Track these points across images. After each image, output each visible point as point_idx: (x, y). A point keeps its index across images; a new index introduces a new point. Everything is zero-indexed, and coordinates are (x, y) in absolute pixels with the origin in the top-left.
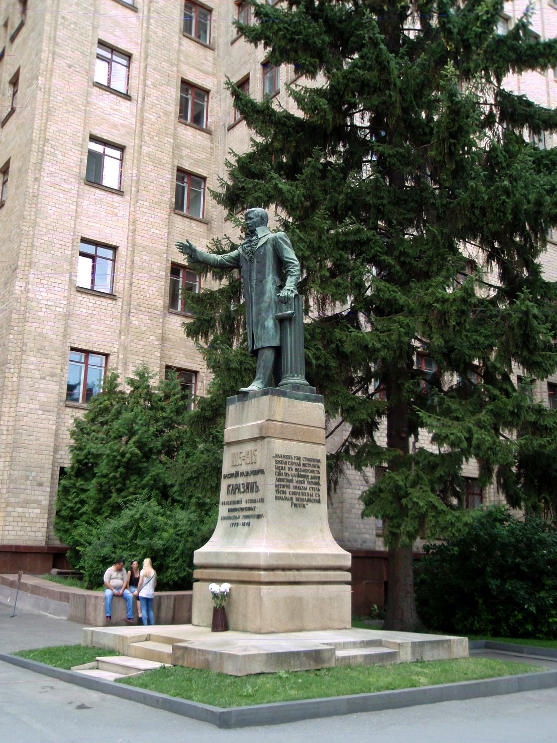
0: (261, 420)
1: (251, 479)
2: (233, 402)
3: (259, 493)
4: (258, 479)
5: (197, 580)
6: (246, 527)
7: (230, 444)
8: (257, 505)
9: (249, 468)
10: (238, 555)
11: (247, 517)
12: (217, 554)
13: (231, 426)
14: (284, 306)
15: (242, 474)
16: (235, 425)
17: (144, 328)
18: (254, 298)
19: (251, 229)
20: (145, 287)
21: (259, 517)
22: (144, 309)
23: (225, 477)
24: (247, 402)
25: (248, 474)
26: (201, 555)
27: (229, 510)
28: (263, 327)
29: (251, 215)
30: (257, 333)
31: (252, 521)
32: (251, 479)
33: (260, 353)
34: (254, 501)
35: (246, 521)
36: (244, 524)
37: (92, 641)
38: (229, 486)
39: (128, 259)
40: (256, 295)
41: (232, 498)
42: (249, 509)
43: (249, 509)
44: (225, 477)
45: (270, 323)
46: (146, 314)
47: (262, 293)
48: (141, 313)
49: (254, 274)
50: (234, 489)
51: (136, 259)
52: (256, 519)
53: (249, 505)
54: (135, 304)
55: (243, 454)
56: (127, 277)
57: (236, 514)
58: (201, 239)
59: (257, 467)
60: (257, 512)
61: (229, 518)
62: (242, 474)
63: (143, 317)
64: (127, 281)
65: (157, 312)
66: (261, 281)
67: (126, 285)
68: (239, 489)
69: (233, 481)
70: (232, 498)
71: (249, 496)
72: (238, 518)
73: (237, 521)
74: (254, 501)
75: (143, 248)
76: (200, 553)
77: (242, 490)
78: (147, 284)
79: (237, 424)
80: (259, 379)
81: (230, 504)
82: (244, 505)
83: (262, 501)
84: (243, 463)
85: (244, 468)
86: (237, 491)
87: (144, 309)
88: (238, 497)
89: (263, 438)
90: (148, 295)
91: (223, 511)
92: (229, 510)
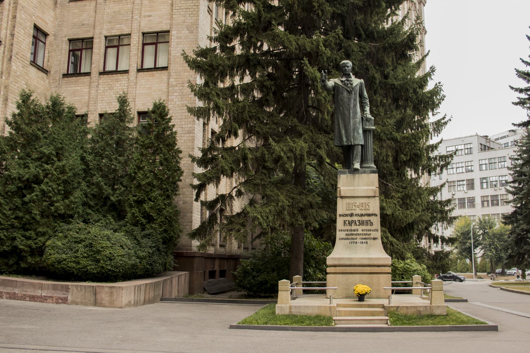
0: (371, 186)
1: (365, 218)
2: (344, 173)
3: (373, 226)
4: (372, 218)
5: (329, 273)
6: (364, 245)
7: (342, 197)
8: (371, 232)
9: (363, 212)
10: (370, 259)
11: (365, 239)
12: (350, 259)
13: (343, 186)
14: (368, 124)
15: (357, 215)
16: (346, 187)
17: (19, 73)
18: (351, 114)
19: (347, 73)
20: (21, 40)
21: (374, 239)
22: (20, 58)
23: (340, 215)
24: (357, 175)
25: (362, 215)
26: (330, 259)
27: (346, 235)
28: (358, 133)
29: (348, 65)
30: (354, 135)
31: (368, 241)
32: (365, 218)
33: (356, 147)
34: (370, 230)
35: (364, 241)
36: (362, 243)
37: (290, 312)
38: (345, 222)
39: (11, 13)
40: (353, 113)
41: (349, 228)
42: (365, 235)
43: (365, 235)
44: (340, 215)
45: (361, 131)
46: (21, 61)
47: (355, 113)
48: (18, 60)
49: (352, 101)
50: (350, 223)
51: (18, 15)
52: (372, 240)
53: (365, 232)
54: (15, 52)
55: (358, 204)
56: (9, 28)
57: (354, 237)
58: (50, 10)
59: (370, 212)
60: (372, 236)
61: (347, 239)
62: (357, 215)
63: (18, 64)
64: (9, 32)
65: (26, 62)
66: (355, 106)
67: (8, 35)
68: (356, 223)
69: (349, 218)
70: (349, 228)
71: (364, 227)
72: (356, 239)
73: (355, 241)
74: (370, 230)
75: (23, 7)
76: (333, 258)
77: (357, 223)
78: (23, 37)
79: (350, 186)
80: (358, 162)
81: (348, 230)
82: (360, 232)
83: (377, 230)
84: (358, 209)
85: (358, 212)
86: (353, 224)
87: (20, 58)
88: (354, 227)
89: (375, 197)
90: (22, 47)
91: (339, 235)
92: (346, 235)
